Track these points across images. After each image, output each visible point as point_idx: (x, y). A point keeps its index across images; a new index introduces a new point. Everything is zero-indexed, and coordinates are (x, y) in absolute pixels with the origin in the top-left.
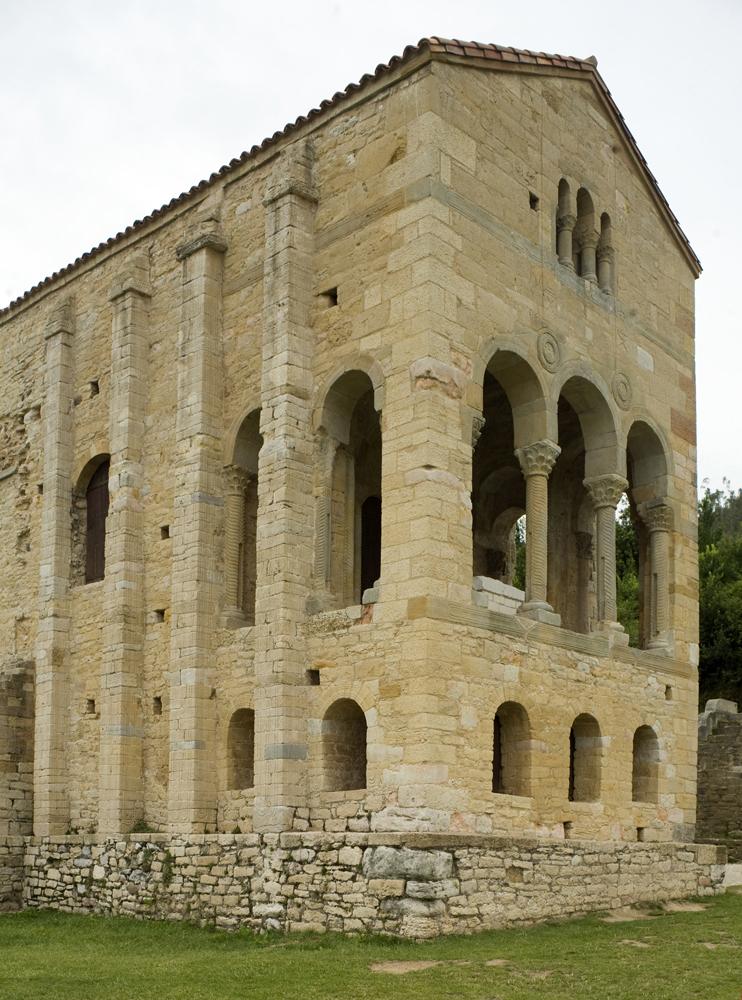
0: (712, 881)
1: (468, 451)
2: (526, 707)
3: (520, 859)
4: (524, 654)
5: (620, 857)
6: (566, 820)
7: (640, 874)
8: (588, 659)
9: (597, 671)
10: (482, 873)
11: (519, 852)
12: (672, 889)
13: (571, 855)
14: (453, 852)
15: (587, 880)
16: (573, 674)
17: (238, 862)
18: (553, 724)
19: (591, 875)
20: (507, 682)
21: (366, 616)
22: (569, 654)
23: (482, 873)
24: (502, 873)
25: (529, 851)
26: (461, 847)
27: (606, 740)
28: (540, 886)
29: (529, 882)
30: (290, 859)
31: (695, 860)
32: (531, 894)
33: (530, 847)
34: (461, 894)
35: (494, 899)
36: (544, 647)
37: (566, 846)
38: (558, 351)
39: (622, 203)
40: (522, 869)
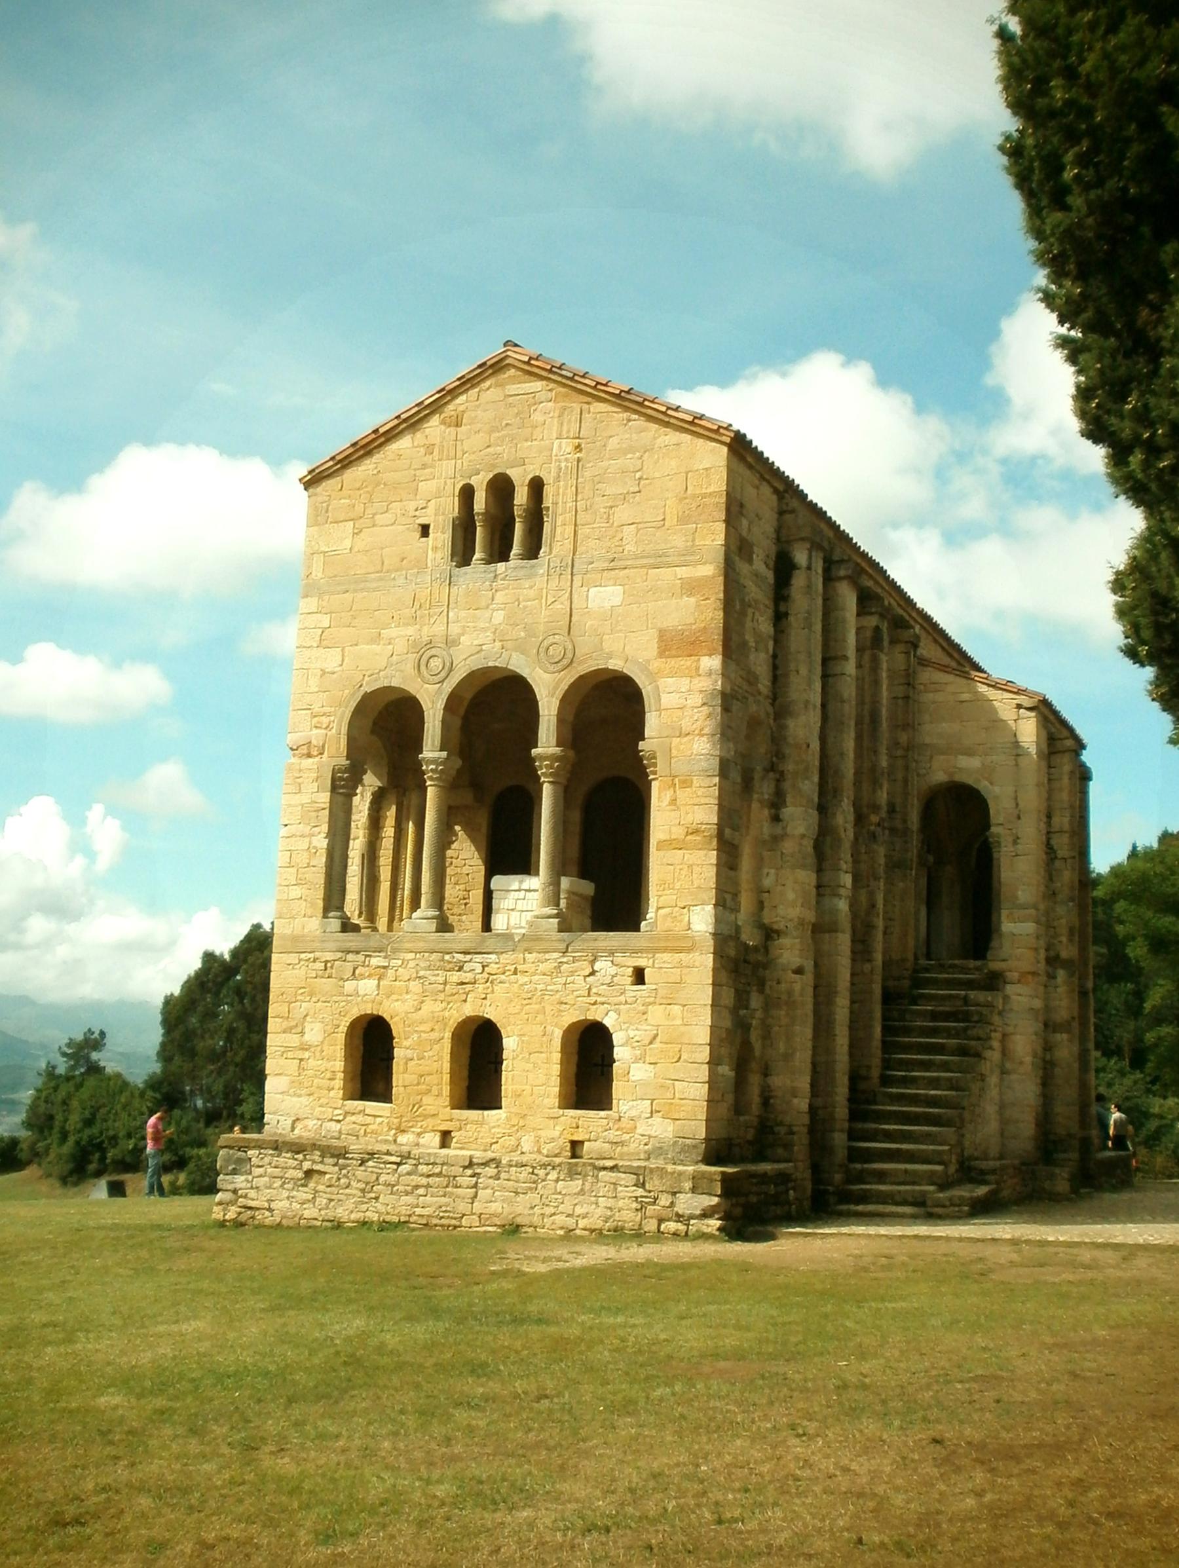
0: (678, 1215)
1: (325, 797)
2: (388, 1019)
3: (322, 1162)
4: (385, 967)
5: (478, 1171)
6: (444, 1127)
7: (517, 1193)
8: (478, 958)
9: (493, 968)
11: (322, 1156)
13: (398, 1164)
15: (421, 1191)
16: (455, 977)
18: (424, 1032)
19: (428, 1186)
20: (365, 995)
22: (447, 957)
24: (301, 1175)
25: (333, 1156)
27: (509, 1043)
28: (347, 1191)
32: (333, 1197)
33: (340, 1154)
34: (252, 1188)
35: (288, 1198)
37: (388, 1153)
40: (325, 1173)
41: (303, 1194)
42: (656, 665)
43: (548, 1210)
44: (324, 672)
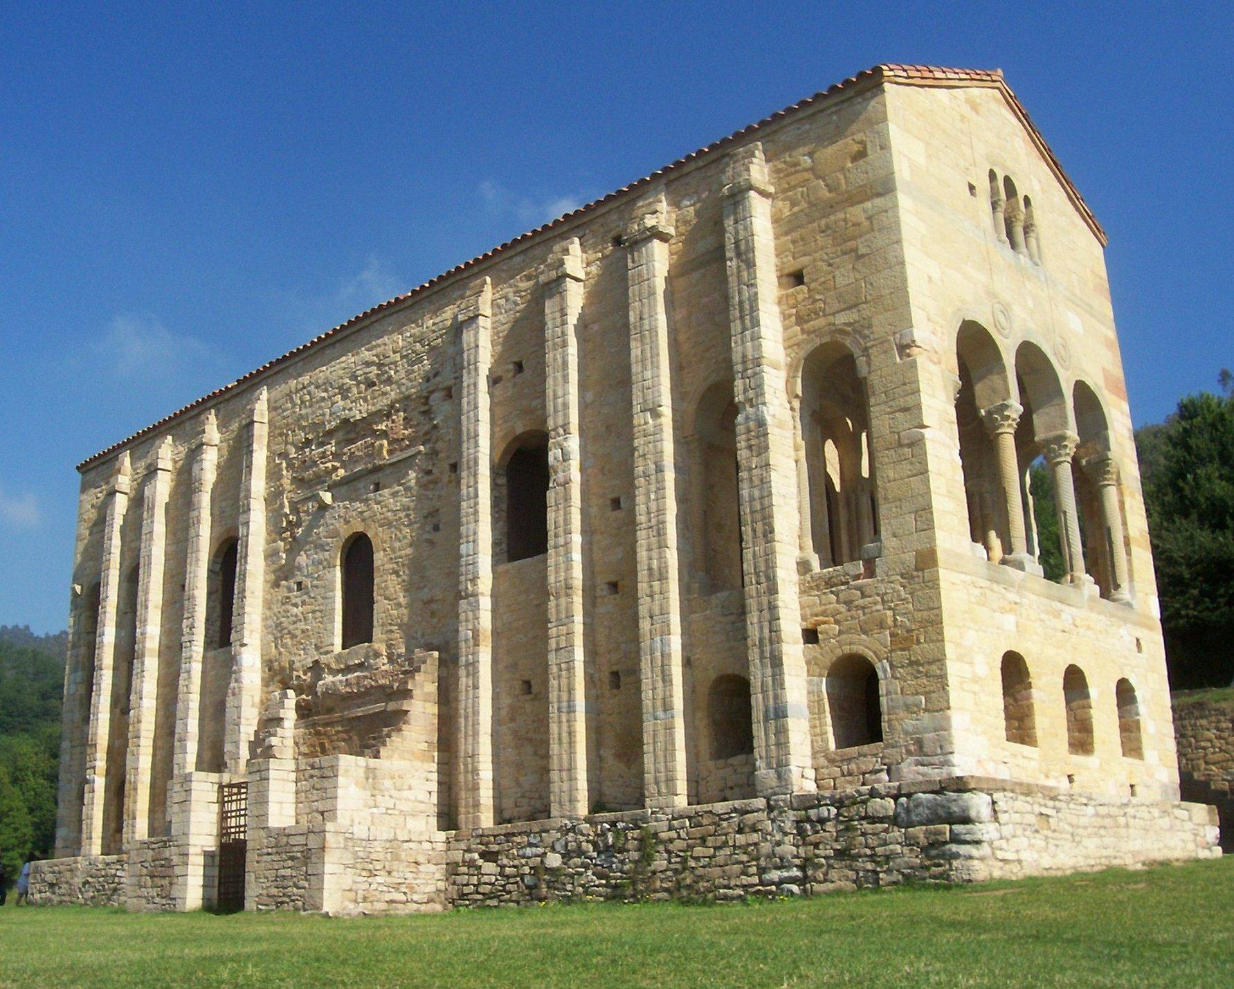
3: (1045, 806)
9: (1078, 622)
10: (1016, 817)
12: (1175, 849)
14: (991, 795)
17: (740, 831)
21: (870, 573)
23: (1016, 817)
25: (1052, 799)
26: (997, 790)
28: (1064, 836)
29: (1055, 831)
30: (809, 820)
31: (1190, 819)
36: (1033, 597)
38: (1008, 318)
39: (1037, 187)
41: (1039, 842)
42: (1106, 392)
43: (1161, 845)
44: (930, 277)
